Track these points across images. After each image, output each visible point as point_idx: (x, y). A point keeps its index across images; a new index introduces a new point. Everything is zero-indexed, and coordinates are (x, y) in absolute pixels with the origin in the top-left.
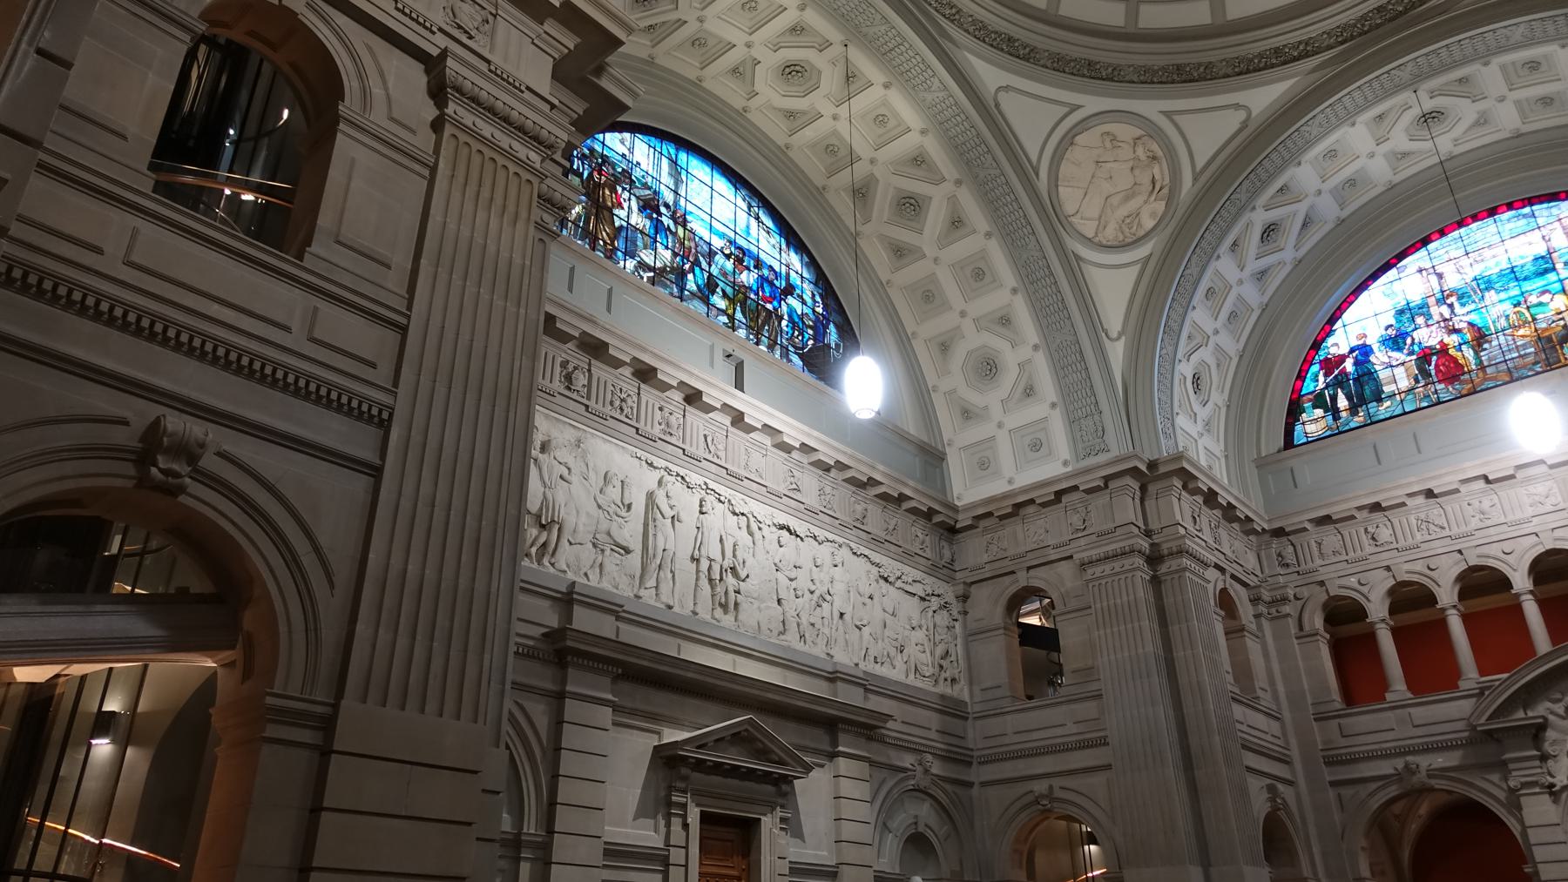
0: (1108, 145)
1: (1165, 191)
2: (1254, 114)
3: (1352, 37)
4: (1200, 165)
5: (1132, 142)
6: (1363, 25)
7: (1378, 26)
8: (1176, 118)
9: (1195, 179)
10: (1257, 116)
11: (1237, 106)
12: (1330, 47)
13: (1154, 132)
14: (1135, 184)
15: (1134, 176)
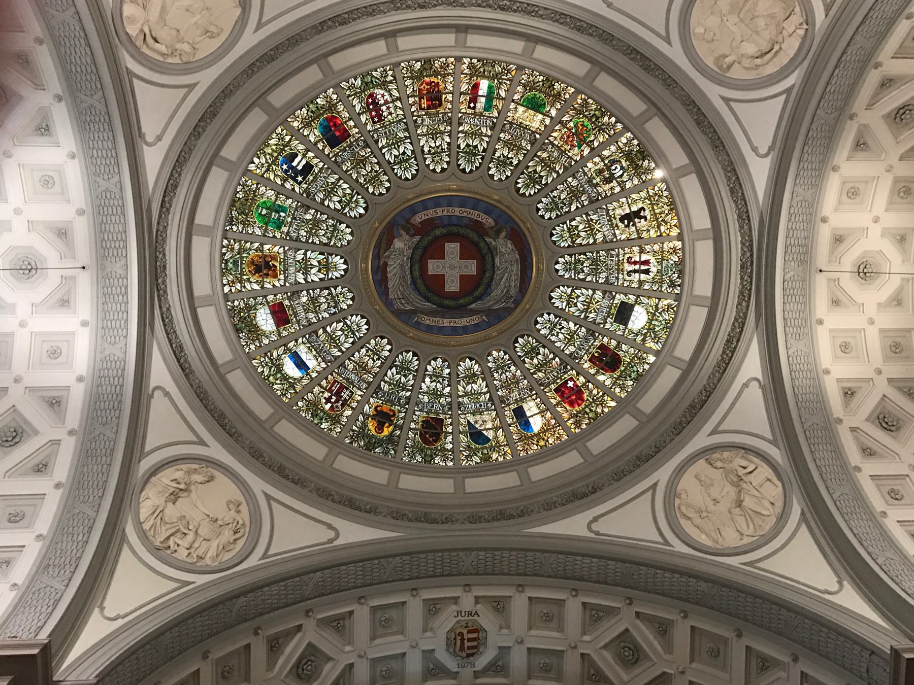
0: (213, 28)
1: (139, 43)
2: (145, 147)
3: (157, 242)
4: (136, 82)
5: (196, 46)
6: (160, 252)
7: (156, 262)
8: (185, 90)
9: (129, 72)
10: (142, 147)
11: (159, 138)
12: (158, 223)
13: (188, 68)
14: (165, 25)
15: (171, 29)
